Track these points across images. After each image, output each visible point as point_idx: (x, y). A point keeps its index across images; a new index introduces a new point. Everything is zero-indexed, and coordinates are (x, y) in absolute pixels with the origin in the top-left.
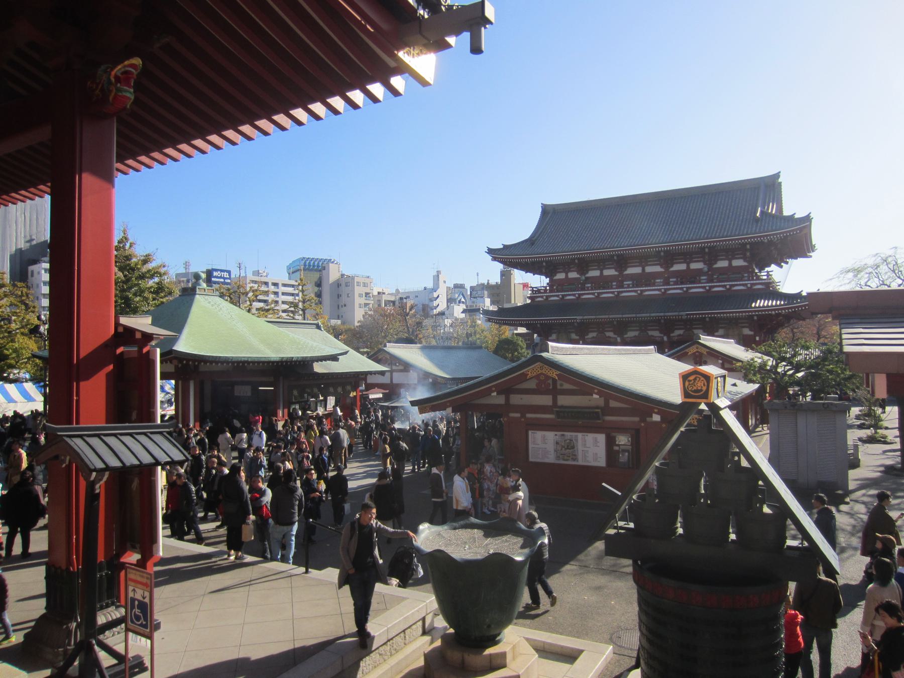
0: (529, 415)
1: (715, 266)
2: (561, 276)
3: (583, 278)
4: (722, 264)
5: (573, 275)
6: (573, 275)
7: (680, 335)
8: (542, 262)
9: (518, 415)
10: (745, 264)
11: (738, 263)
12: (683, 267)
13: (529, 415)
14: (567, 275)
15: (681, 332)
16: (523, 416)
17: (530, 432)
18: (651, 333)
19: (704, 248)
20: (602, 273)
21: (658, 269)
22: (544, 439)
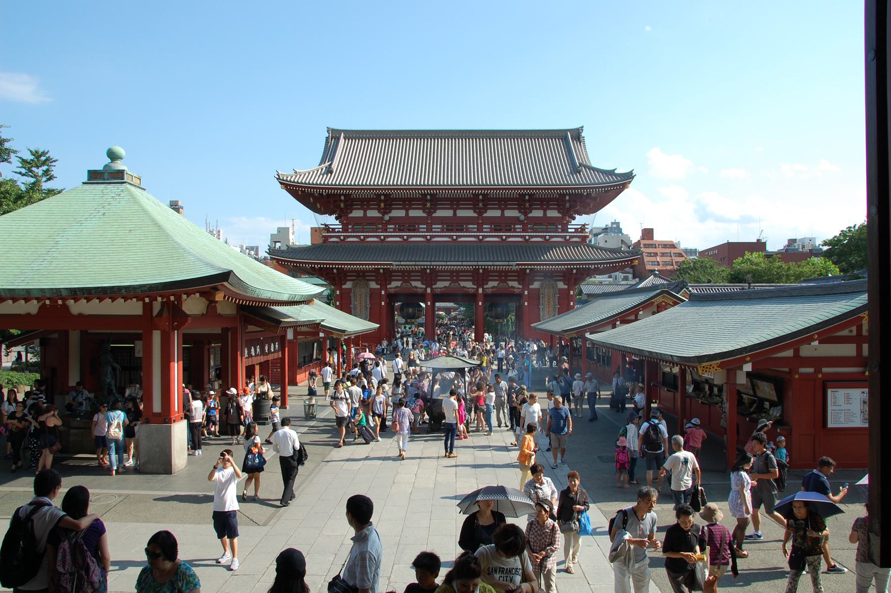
0: (825, 370)
1: (530, 215)
2: (357, 213)
3: (387, 217)
4: (537, 213)
5: (373, 213)
6: (373, 213)
7: (493, 287)
8: (340, 195)
9: (811, 370)
10: (560, 215)
11: (553, 213)
12: (497, 213)
13: (825, 370)
14: (365, 214)
15: (495, 284)
16: (818, 371)
17: (829, 391)
18: (462, 284)
19: (478, 195)
20: (407, 214)
21: (470, 213)
22: (848, 398)
